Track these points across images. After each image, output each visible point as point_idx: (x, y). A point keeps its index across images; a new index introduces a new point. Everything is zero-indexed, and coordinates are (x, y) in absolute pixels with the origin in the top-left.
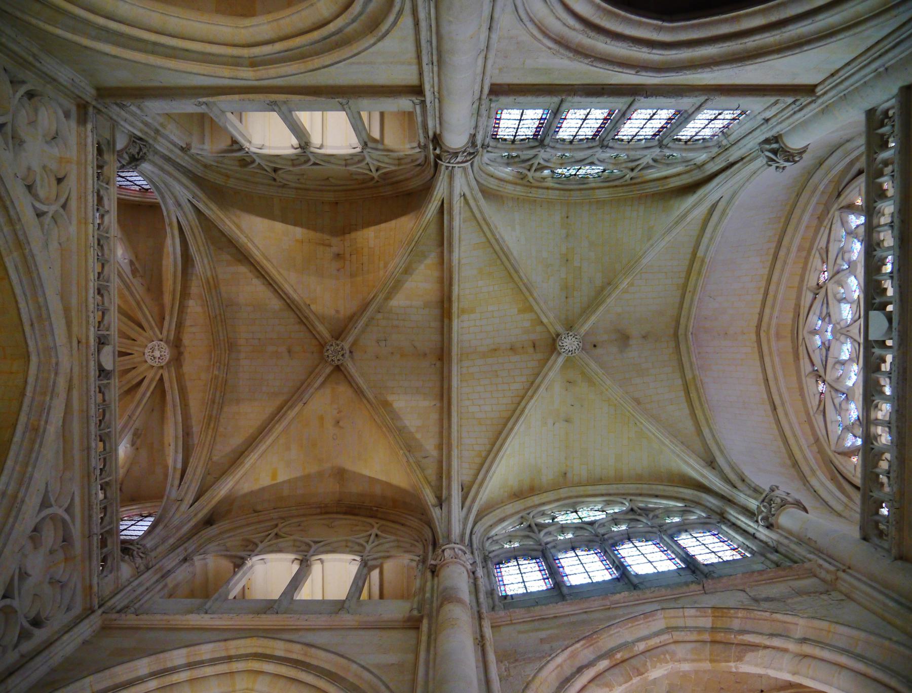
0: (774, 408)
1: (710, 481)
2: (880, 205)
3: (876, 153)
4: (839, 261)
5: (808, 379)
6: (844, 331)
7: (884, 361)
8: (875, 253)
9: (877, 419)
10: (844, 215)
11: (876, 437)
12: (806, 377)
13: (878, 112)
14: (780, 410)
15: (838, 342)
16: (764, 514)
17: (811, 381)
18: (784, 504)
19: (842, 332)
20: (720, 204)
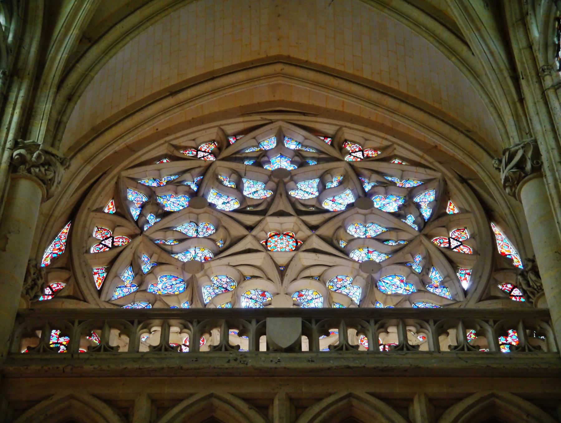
0: (173, 92)
1: (61, 42)
2: (430, 329)
3: (495, 322)
4: (375, 177)
5: (216, 129)
6: (281, 189)
7: (240, 335)
8: (372, 322)
9: (169, 326)
10: (436, 184)
11: (147, 328)
12: (219, 127)
13: (545, 325)
14: (170, 101)
15: (266, 178)
16: (28, 157)
17: (213, 133)
18: (47, 183)
19: (280, 182)
20: (465, 48)
